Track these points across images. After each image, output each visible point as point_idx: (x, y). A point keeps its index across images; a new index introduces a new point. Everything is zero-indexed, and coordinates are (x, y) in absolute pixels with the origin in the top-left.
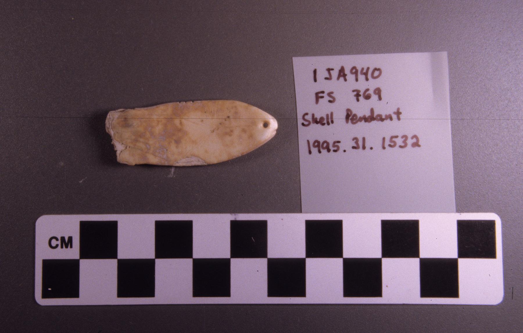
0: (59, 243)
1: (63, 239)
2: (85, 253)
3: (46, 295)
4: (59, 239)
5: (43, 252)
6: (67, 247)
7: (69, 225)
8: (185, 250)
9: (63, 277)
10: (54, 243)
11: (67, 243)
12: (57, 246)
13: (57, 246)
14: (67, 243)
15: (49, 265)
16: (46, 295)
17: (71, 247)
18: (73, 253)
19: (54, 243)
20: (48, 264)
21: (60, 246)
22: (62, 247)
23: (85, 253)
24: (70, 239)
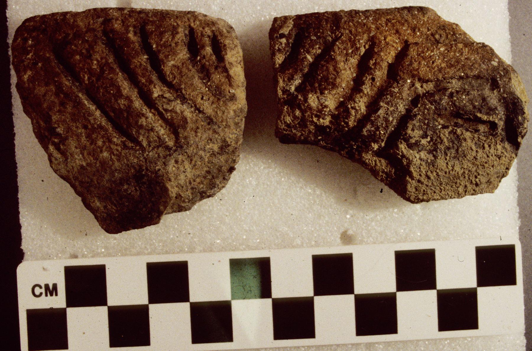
0: (43, 290)
1: (47, 286)
5: (26, 302)
6: (51, 295)
8: (181, 295)
10: (37, 291)
11: (51, 290)
12: (41, 294)
13: (41, 294)
14: (51, 290)
17: (56, 295)
18: (59, 301)
21: (44, 294)
22: (46, 295)
23: (74, 300)
24: (55, 286)
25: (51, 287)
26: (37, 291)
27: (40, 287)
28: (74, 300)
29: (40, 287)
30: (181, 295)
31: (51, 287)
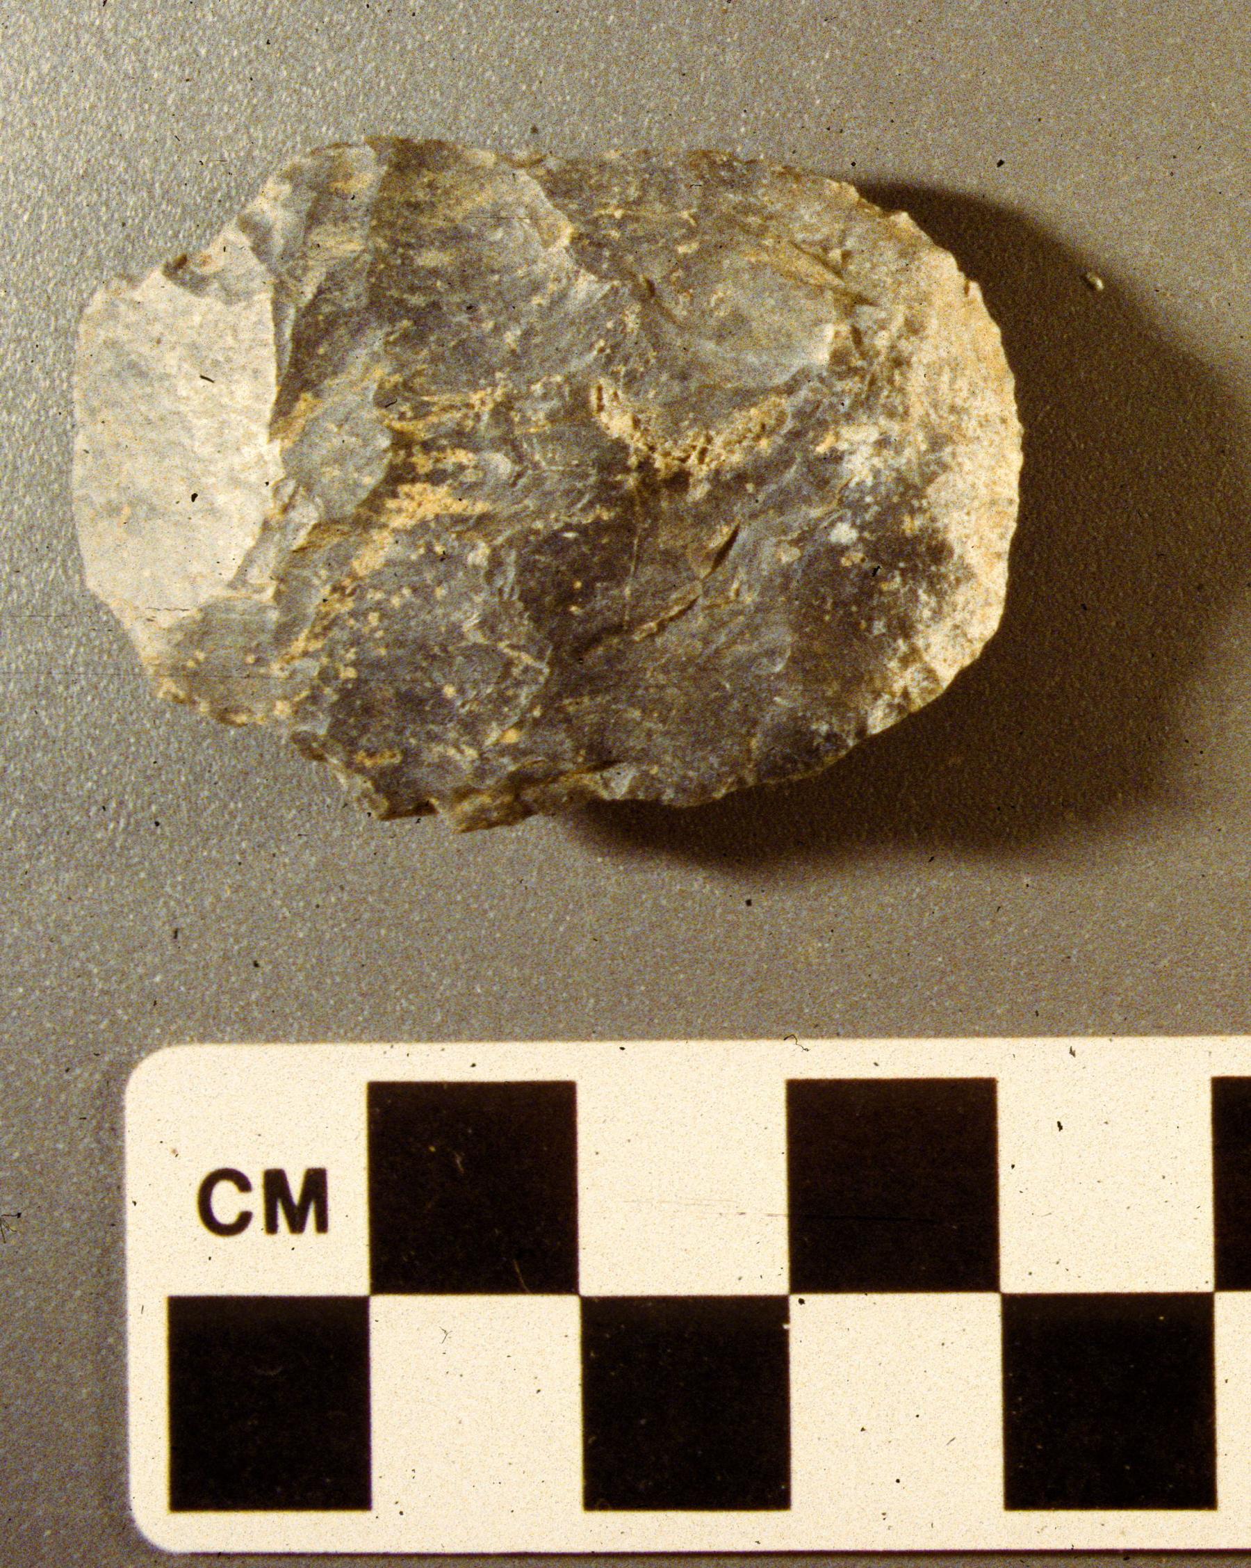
0: (255, 1201)
1: (275, 1182)
2: (398, 1266)
3: (186, 1495)
4: (257, 1182)
6: (297, 1226)
7: (306, 1103)
8: (963, 1255)
11: (297, 1202)
13: (245, 1219)
14: (297, 1202)
15: (201, 1328)
16: (186, 1495)
17: (322, 1226)
18: (331, 1261)
19: (227, 1203)
20: (193, 1321)
21: (258, 1221)
22: (272, 1227)
24: (316, 1182)
25: (296, 1188)
26: (227, 1203)
27: (243, 1184)
29: (243, 1184)
30: (963, 1255)
31: (296, 1188)
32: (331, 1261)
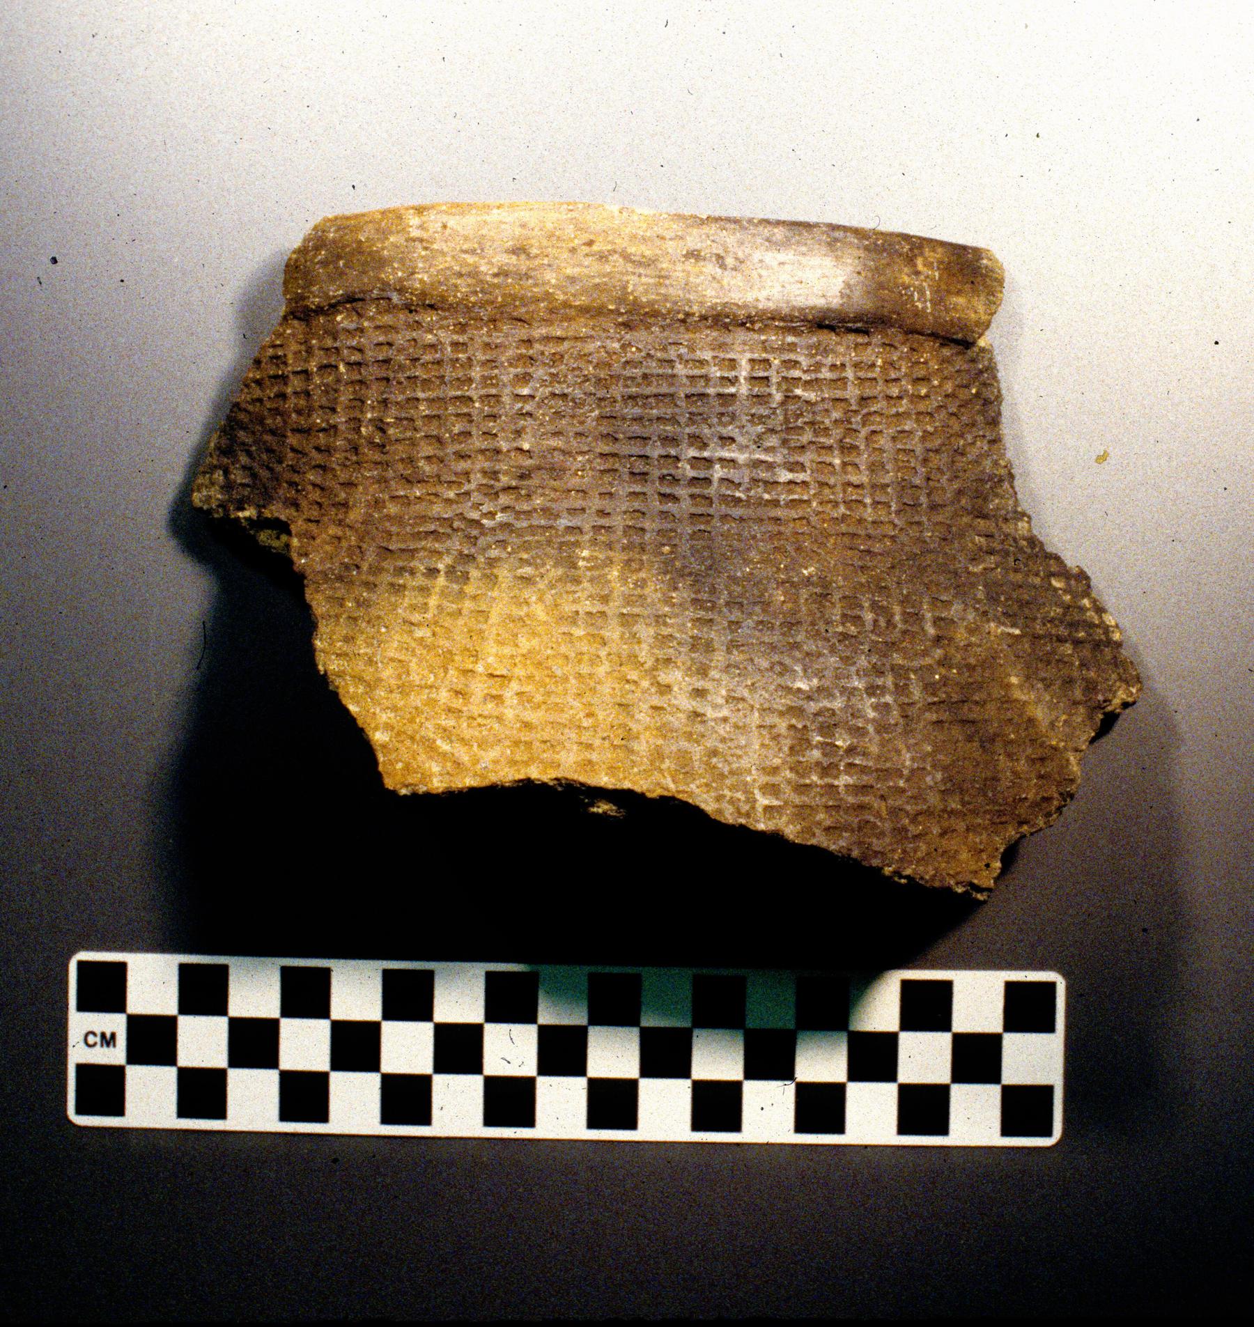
0: (98, 1039)
1: (103, 1035)
6: (108, 1045)
9: (104, 1088)
10: (91, 1039)
11: (108, 1040)
12: (95, 1044)
13: (95, 1044)
14: (108, 1040)
15: (84, 1070)
18: (116, 1055)
20: (80, 1068)
23: (135, 1056)
24: (113, 1035)
25: (108, 1036)
26: (91, 1039)
27: (94, 1034)
28: (135, 1056)
29: (94, 1034)
31: (108, 1036)
32: (116, 1055)
